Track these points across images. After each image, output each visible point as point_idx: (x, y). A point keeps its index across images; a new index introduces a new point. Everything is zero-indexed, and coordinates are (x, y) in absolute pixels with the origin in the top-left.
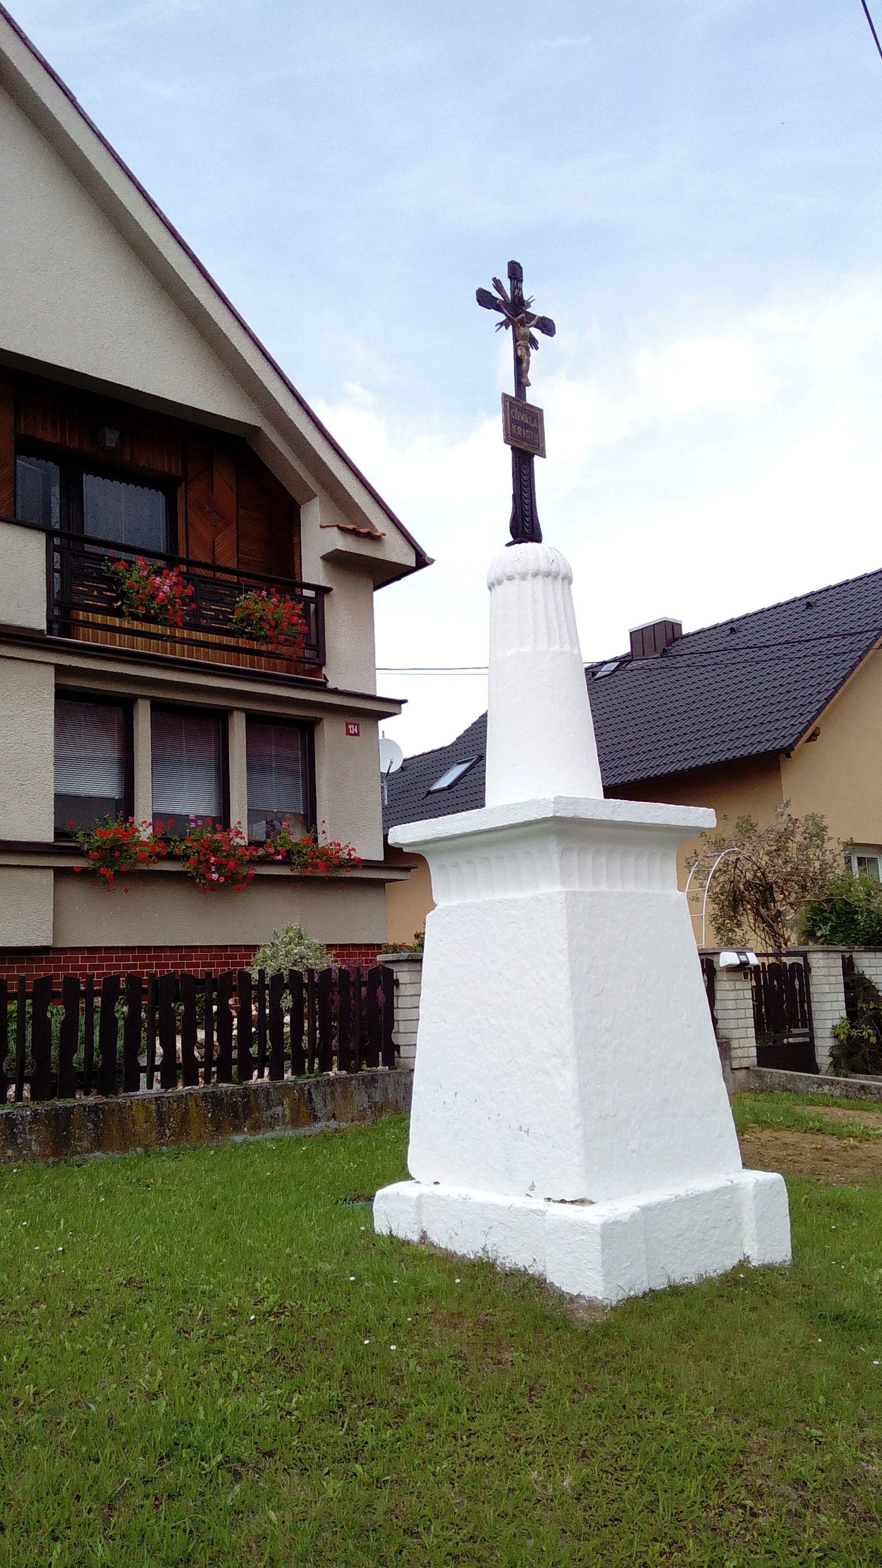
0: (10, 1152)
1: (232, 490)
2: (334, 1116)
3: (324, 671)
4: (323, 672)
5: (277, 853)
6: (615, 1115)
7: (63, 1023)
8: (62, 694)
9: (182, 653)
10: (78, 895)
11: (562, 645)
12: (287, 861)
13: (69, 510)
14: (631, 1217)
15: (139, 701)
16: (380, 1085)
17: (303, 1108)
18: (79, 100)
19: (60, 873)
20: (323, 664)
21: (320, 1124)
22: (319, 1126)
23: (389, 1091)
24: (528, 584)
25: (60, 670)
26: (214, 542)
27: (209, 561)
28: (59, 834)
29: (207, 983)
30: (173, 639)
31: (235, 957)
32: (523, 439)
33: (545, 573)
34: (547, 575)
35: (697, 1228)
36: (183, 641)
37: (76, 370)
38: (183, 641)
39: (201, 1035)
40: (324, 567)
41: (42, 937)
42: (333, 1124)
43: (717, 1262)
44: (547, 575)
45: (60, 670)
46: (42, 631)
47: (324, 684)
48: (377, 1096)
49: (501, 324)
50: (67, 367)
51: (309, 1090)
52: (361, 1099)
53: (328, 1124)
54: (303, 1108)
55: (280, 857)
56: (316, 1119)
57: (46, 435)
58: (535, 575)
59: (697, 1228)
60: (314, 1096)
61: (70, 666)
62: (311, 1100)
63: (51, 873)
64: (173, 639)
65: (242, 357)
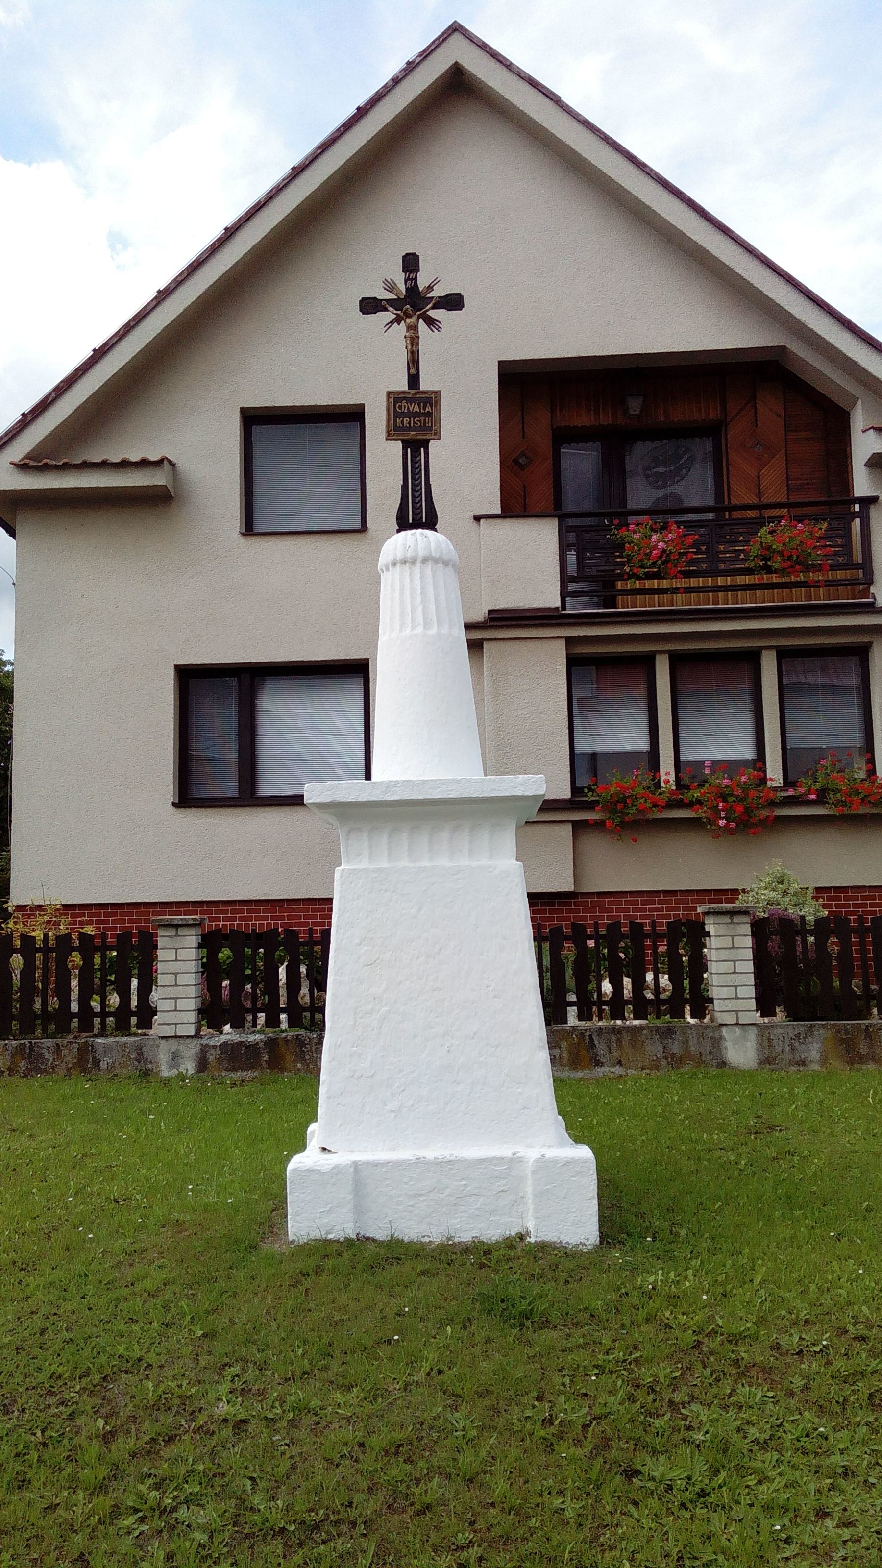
0: (299, 1065)
1: (778, 415)
2: (620, 1063)
3: (873, 590)
4: (872, 591)
5: (809, 792)
6: (372, 1076)
7: (575, 962)
8: (573, 662)
9: (680, 603)
10: (598, 848)
11: (413, 627)
12: (821, 800)
13: (610, 486)
14: (334, 1168)
15: (657, 656)
16: (679, 1036)
17: (583, 1052)
18: (567, 98)
19: (577, 826)
20: (870, 582)
21: (603, 1069)
22: (600, 1071)
23: (691, 1043)
24: (429, 568)
25: (569, 641)
26: (759, 476)
27: (754, 501)
28: (575, 790)
29: (268, 939)
30: (716, 589)
31: (299, 917)
32: (410, 429)
33: (401, 560)
34: (404, 562)
35: (448, 1191)
36: (725, 589)
37: (583, 355)
38: (725, 589)
39: (649, 977)
40: (870, 474)
41: (567, 886)
42: (618, 1070)
43: (493, 1230)
44: (404, 562)
45: (569, 641)
46: (557, 608)
47: (872, 604)
48: (676, 1048)
49: (392, 322)
50: (574, 355)
51: (590, 1036)
52: (654, 1049)
53: (613, 1070)
54: (583, 1052)
55: (813, 797)
56: (599, 1064)
57: (583, 420)
58: (394, 564)
59: (448, 1191)
60: (596, 1042)
61: (579, 636)
62: (593, 1046)
63: (569, 827)
64: (716, 589)
65: (749, 282)
